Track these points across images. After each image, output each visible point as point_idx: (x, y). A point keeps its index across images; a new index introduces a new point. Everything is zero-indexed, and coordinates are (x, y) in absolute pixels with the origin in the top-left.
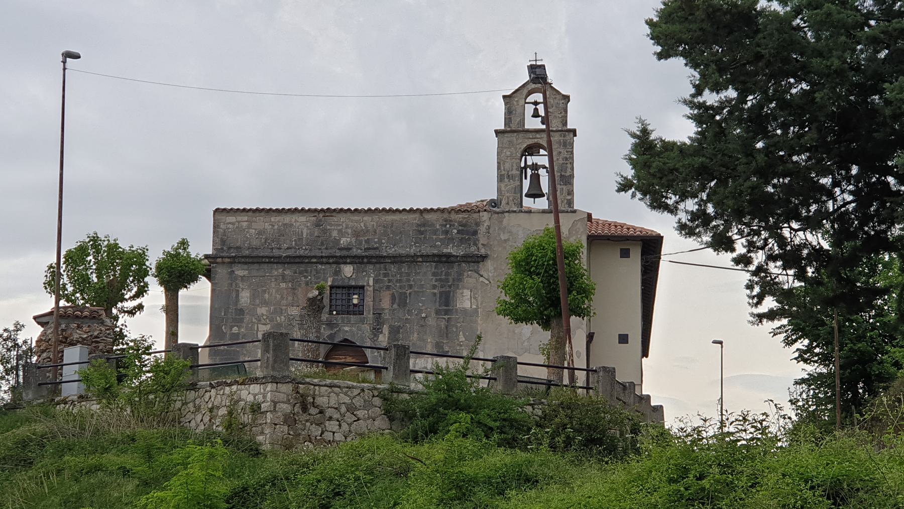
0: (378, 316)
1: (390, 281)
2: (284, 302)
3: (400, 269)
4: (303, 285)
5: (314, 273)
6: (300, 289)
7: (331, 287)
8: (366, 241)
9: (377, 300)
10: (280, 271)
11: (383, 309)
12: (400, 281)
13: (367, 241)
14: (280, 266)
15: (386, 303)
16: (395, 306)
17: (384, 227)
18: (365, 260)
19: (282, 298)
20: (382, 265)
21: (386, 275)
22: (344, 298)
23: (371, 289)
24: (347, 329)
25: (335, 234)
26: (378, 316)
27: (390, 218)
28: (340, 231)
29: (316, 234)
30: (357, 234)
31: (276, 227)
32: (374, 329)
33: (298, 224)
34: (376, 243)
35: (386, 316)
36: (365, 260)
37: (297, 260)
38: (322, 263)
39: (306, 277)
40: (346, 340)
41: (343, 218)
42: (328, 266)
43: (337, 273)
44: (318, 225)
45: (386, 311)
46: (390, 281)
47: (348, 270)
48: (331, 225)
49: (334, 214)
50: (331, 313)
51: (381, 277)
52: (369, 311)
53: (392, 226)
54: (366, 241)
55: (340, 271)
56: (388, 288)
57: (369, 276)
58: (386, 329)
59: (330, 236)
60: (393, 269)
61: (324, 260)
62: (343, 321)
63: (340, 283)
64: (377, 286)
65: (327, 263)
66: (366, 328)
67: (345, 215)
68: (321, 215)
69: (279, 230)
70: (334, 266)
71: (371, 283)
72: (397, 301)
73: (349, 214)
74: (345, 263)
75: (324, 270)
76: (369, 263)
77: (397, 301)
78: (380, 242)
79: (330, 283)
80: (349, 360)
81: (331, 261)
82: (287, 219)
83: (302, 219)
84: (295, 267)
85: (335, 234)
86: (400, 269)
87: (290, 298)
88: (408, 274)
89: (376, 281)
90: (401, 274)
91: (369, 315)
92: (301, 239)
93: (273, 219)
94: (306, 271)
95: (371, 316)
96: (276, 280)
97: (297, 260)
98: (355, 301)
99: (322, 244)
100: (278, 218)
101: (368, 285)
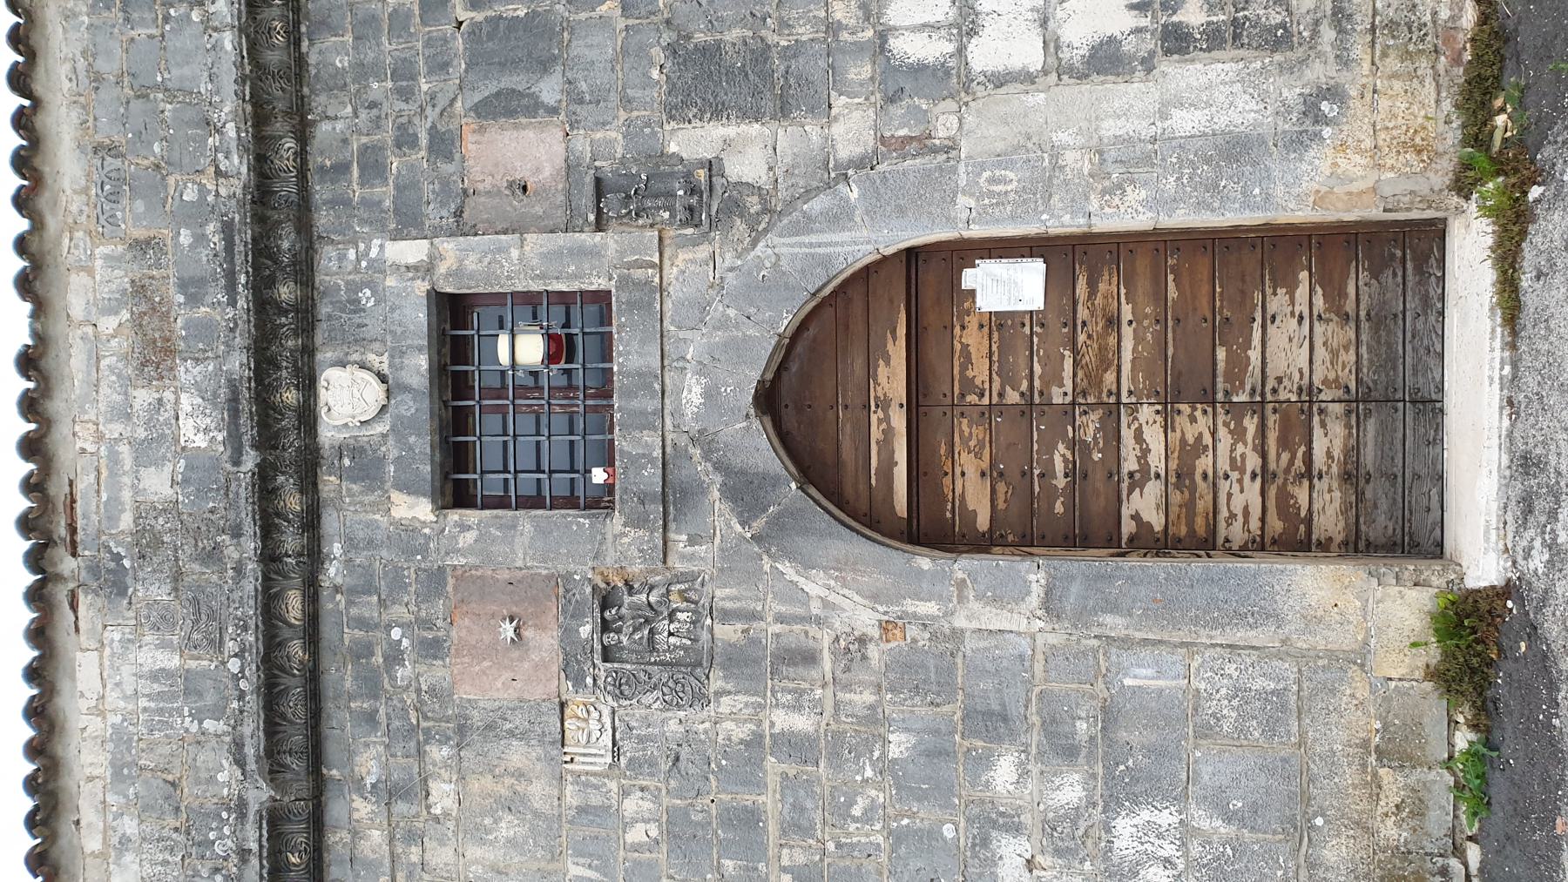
0: (608, 197)
1: (405, 140)
2: (538, 791)
3: (337, 84)
4: (436, 673)
5: (368, 607)
6: (465, 692)
7: (456, 492)
8: (194, 300)
9: (517, 206)
10: (363, 808)
11: (571, 167)
12: (404, 73)
13: (193, 289)
14: (335, 810)
15: (532, 152)
16: (549, 90)
17: (114, 197)
18: (286, 292)
19: (513, 804)
20: (321, 191)
21: (373, 167)
22: (510, 413)
23: (448, 246)
24: (692, 394)
25: (158, 484)
26: (608, 197)
27: (68, 167)
28: (145, 453)
29: (160, 592)
30: (155, 356)
31: (130, 826)
32: (692, 216)
33: (112, 697)
34: (200, 239)
35: (608, 142)
36: (286, 292)
37: (294, 706)
38: (314, 556)
39: (394, 656)
40: (768, 400)
41: (77, 442)
42: (331, 522)
43: (363, 463)
44: (114, 583)
45: (581, 145)
46: (405, 140)
47: (347, 399)
48: (112, 510)
49: (58, 489)
50: (601, 501)
51: (385, 193)
52: (581, 252)
53: (112, 150)
54: (194, 300)
55: (356, 450)
56: (443, 145)
57: (378, 266)
58: (692, 141)
59: (171, 509)
60: (336, 125)
61: (291, 541)
62: (643, 421)
63: (422, 444)
64: (434, 214)
65: (311, 522)
66: (688, 266)
67: (61, 431)
68: (68, 565)
69: (145, 810)
70: (329, 483)
71: (411, 251)
72: (515, 81)
73: (57, 406)
74: (308, 417)
75: (351, 543)
76: (304, 269)
77: (515, 81)
78: (193, 215)
79: (421, 510)
80: (892, 379)
81: (293, 502)
82: (87, 760)
83: (85, 673)
84: (340, 722)
85: (158, 484)
86: (337, 84)
87: (518, 755)
88: (366, 28)
89: (407, 223)
90: (363, 71)
91: (598, 259)
92: (190, 685)
93: (92, 843)
94: (362, 652)
95: (610, 242)
96: (414, 837)
97: (294, 706)
98: (531, 349)
99: (212, 556)
100: (88, 812)
101: (426, 269)
